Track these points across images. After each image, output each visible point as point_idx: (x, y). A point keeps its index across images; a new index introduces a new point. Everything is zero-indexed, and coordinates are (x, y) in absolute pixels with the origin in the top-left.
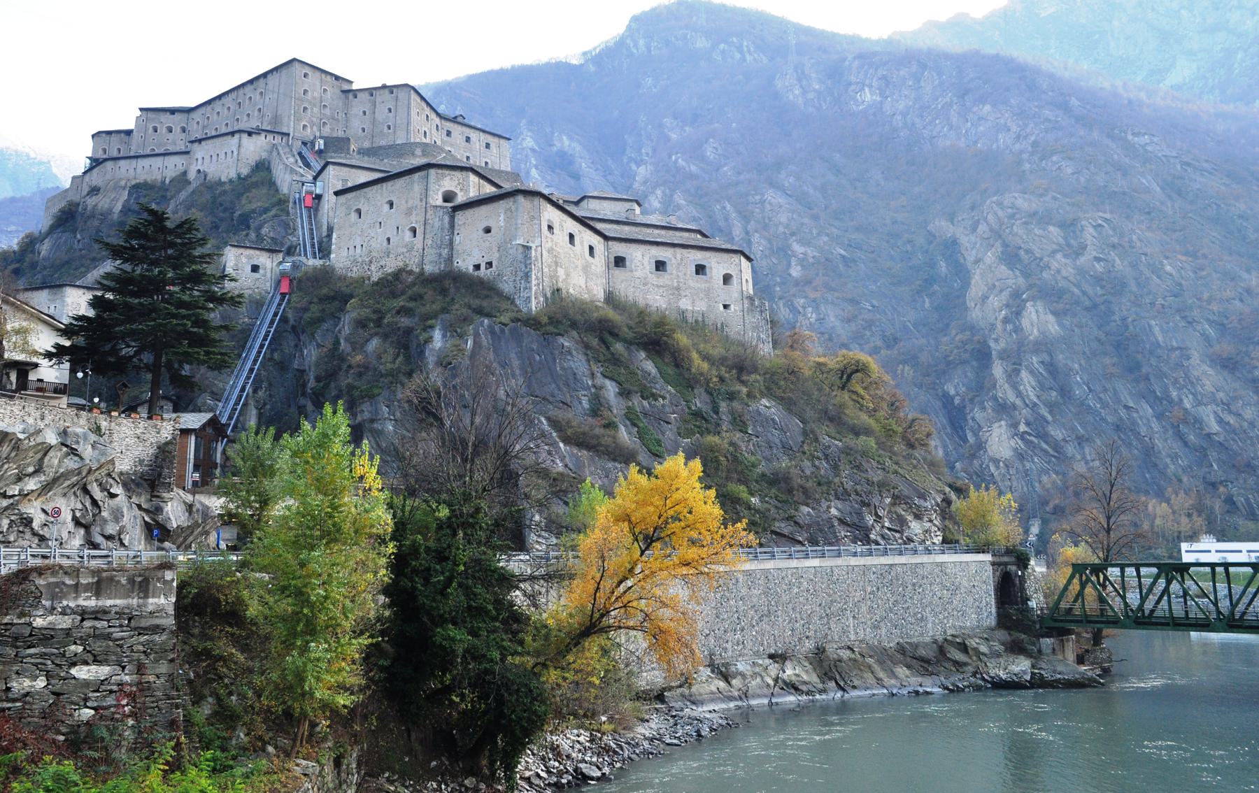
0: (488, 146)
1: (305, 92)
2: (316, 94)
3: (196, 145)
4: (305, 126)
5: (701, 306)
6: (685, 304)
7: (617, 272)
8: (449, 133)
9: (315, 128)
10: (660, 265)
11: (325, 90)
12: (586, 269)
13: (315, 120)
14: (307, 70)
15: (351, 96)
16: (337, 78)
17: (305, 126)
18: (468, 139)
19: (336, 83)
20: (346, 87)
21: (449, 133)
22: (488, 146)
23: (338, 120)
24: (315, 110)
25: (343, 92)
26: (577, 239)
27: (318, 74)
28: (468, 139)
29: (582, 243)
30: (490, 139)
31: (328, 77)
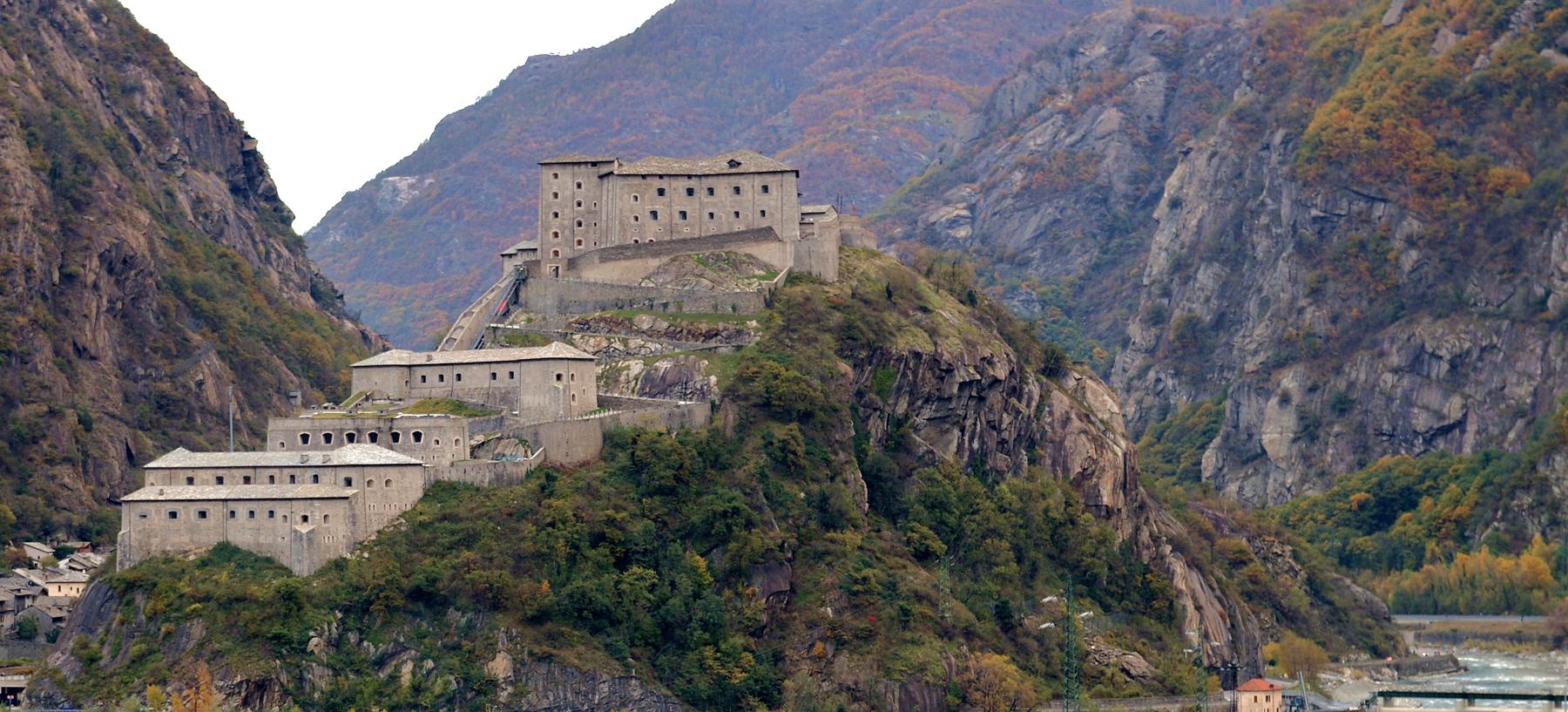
0: (765, 189)
1: (556, 195)
2: (568, 193)
3: (506, 258)
4: (556, 235)
5: (270, 540)
6: (262, 540)
7: (231, 521)
8: (711, 191)
9: (567, 232)
10: (252, 513)
11: (579, 186)
12: (192, 530)
13: (566, 222)
14: (557, 170)
15: (605, 180)
16: (594, 164)
17: (556, 235)
18: (737, 190)
19: (595, 169)
20: (604, 170)
21: (711, 191)
22: (765, 189)
23: (596, 212)
24: (567, 211)
25: (601, 177)
26: (182, 515)
27: (569, 168)
28: (737, 190)
29: (188, 514)
30: (768, 180)
31: (583, 167)
